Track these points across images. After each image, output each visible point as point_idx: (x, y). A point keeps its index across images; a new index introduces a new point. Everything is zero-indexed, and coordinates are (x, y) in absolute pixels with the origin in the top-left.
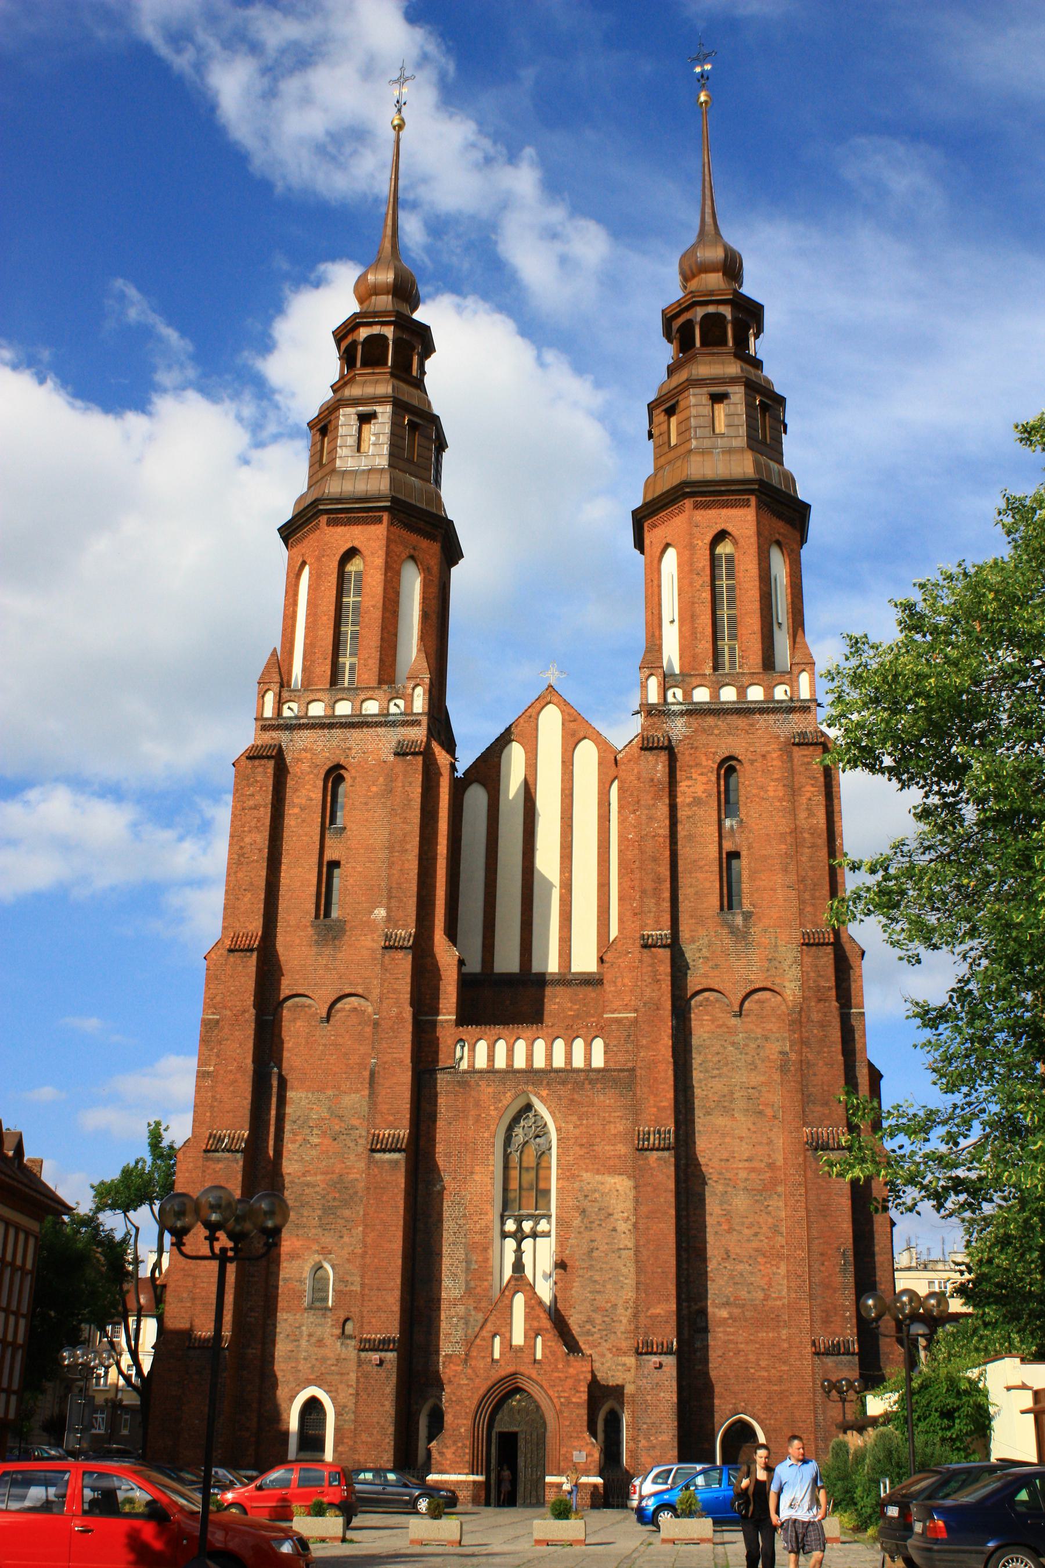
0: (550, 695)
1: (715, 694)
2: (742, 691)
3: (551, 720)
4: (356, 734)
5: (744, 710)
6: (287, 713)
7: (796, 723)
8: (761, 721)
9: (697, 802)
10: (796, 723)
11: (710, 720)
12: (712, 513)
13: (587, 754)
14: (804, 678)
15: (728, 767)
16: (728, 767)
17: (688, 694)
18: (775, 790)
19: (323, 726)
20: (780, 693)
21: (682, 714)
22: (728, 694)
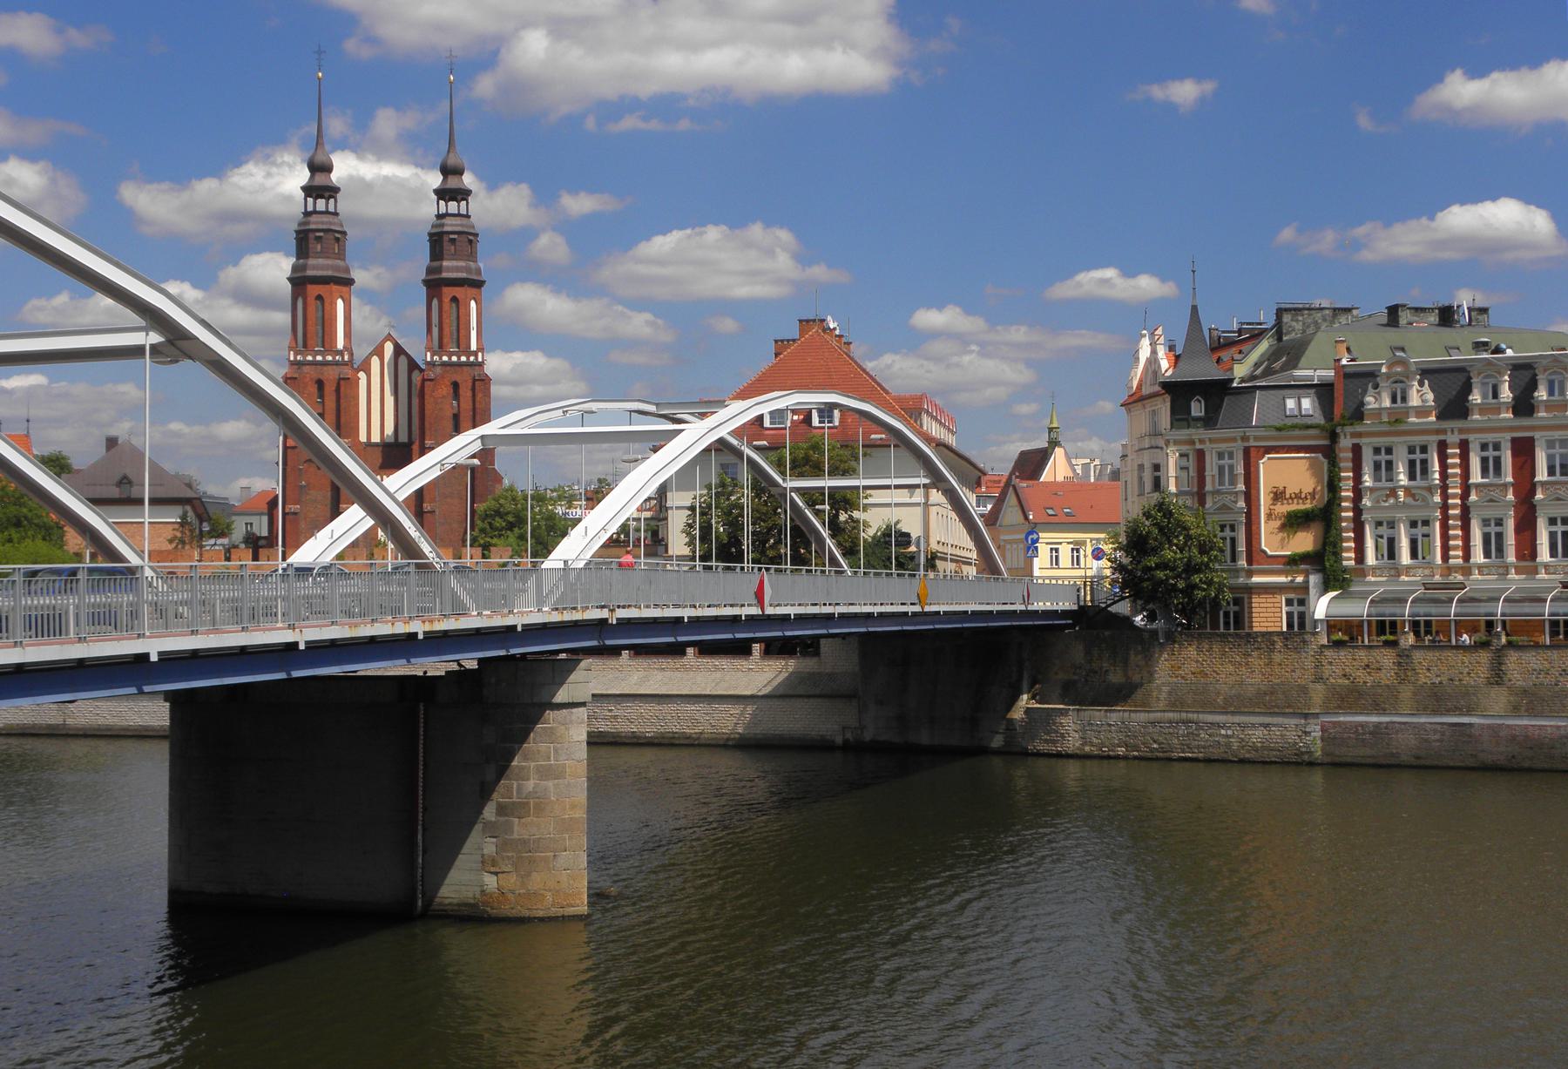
0: (389, 337)
1: (450, 359)
2: (459, 358)
3: (389, 349)
4: (325, 368)
5: (460, 365)
6: (299, 358)
7: (476, 371)
8: (465, 368)
9: (443, 397)
10: (476, 371)
11: (448, 368)
12: (450, 288)
13: (403, 361)
14: (480, 354)
15: (456, 386)
16: (456, 386)
17: (441, 358)
18: (469, 394)
19: (313, 364)
20: (472, 359)
21: (439, 365)
22: (454, 359)
